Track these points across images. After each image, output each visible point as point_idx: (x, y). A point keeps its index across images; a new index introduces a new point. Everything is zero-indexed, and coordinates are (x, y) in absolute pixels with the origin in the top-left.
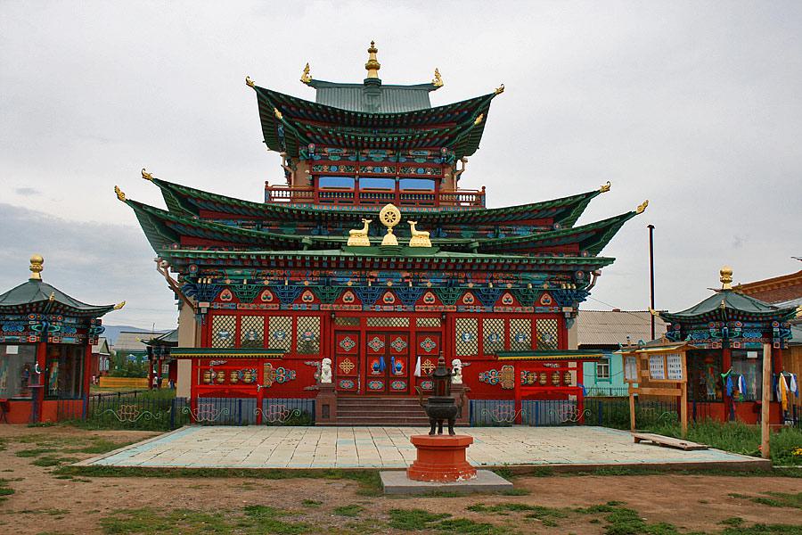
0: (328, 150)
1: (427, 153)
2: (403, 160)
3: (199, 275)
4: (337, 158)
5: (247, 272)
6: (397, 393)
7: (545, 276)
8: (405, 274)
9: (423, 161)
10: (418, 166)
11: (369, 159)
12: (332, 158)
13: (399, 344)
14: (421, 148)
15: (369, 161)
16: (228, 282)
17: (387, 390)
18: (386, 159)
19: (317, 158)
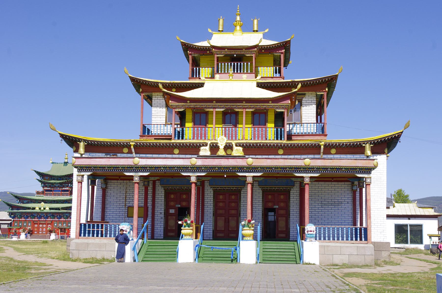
0: (47, 184)
1: (67, 185)
2: (62, 186)
3: (12, 215)
4: (49, 186)
5: (19, 214)
6: (40, 234)
7: (68, 214)
8: (45, 214)
9: (66, 186)
10: (65, 187)
11: (55, 186)
12: (48, 186)
13: (45, 226)
14: (65, 183)
15: (55, 186)
16: (16, 216)
17: (42, 233)
18: (58, 186)
19: (45, 186)
